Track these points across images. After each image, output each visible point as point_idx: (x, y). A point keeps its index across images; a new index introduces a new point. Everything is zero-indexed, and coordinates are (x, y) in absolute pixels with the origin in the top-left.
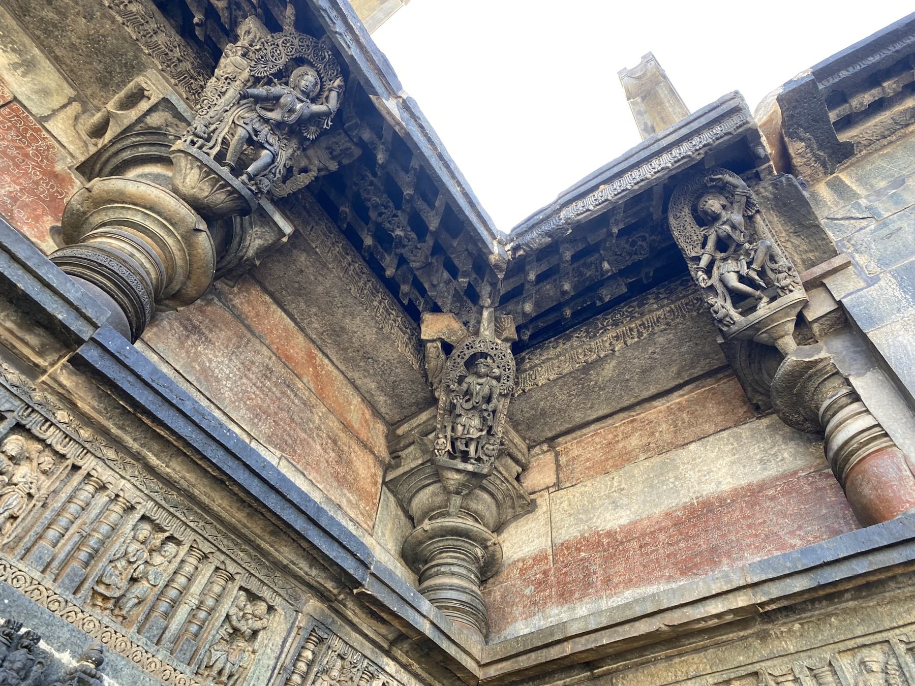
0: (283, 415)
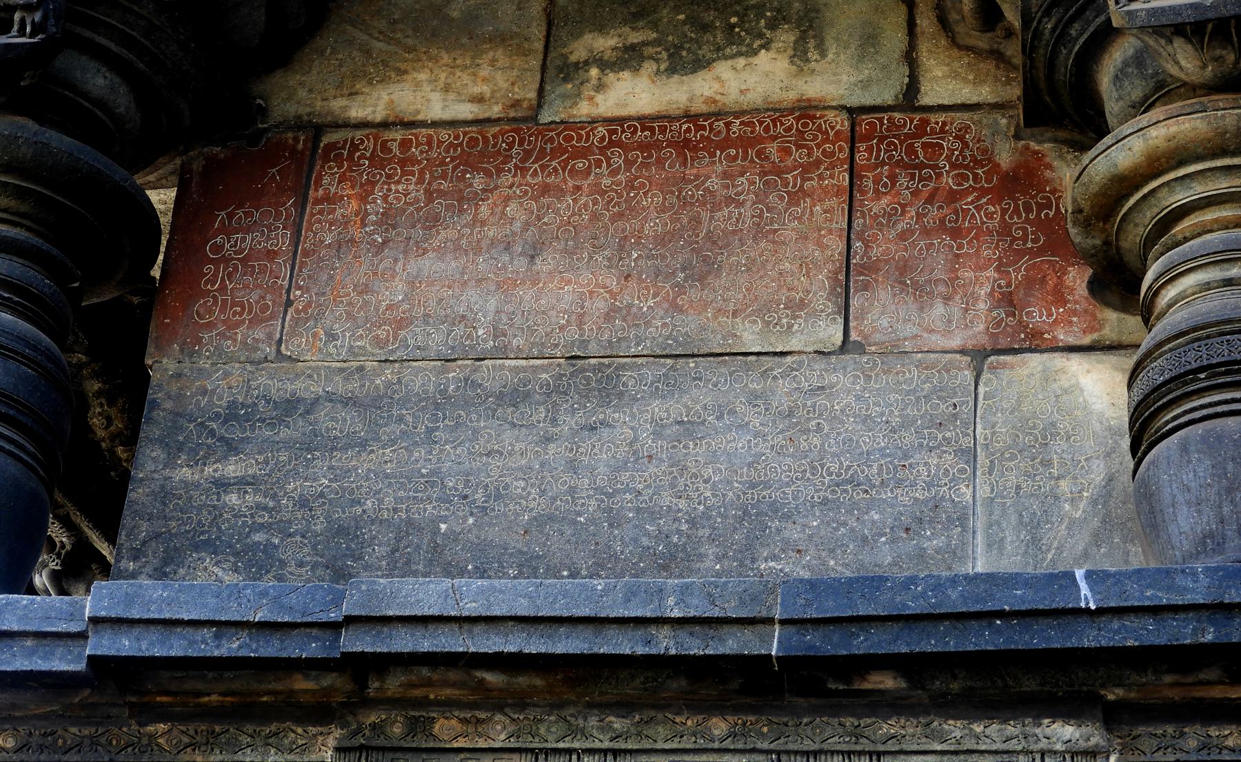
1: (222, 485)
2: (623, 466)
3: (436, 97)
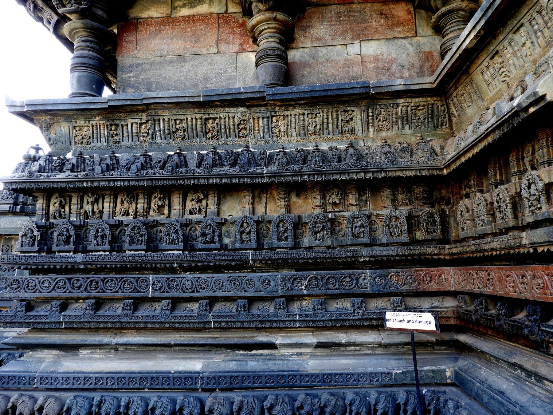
0: (354, 24)
1: (130, 77)
2: (187, 72)
3: (155, 13)
